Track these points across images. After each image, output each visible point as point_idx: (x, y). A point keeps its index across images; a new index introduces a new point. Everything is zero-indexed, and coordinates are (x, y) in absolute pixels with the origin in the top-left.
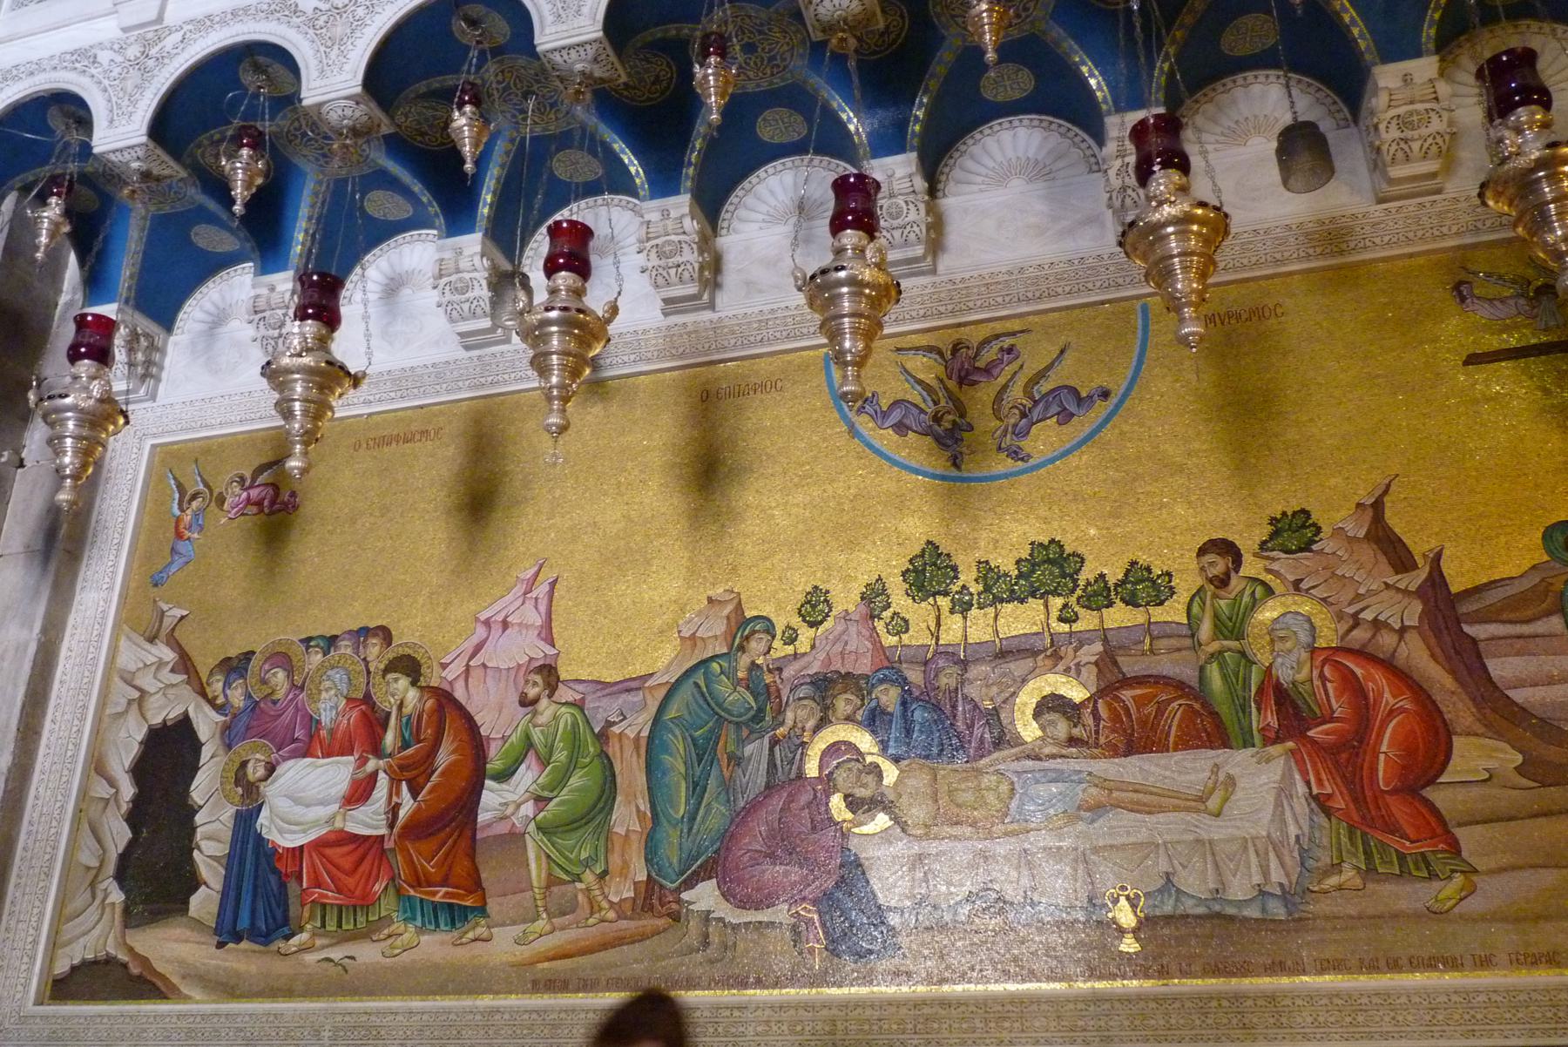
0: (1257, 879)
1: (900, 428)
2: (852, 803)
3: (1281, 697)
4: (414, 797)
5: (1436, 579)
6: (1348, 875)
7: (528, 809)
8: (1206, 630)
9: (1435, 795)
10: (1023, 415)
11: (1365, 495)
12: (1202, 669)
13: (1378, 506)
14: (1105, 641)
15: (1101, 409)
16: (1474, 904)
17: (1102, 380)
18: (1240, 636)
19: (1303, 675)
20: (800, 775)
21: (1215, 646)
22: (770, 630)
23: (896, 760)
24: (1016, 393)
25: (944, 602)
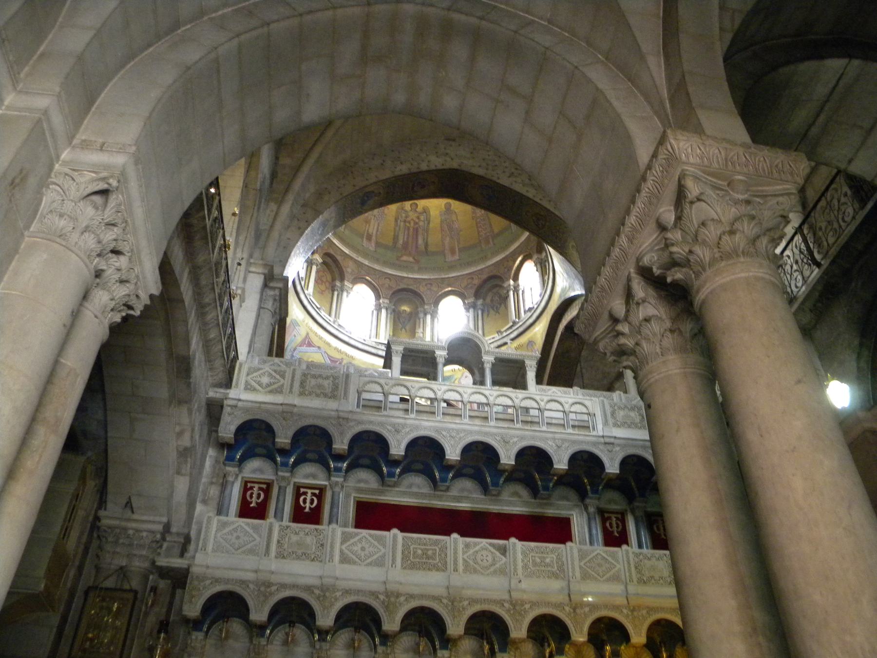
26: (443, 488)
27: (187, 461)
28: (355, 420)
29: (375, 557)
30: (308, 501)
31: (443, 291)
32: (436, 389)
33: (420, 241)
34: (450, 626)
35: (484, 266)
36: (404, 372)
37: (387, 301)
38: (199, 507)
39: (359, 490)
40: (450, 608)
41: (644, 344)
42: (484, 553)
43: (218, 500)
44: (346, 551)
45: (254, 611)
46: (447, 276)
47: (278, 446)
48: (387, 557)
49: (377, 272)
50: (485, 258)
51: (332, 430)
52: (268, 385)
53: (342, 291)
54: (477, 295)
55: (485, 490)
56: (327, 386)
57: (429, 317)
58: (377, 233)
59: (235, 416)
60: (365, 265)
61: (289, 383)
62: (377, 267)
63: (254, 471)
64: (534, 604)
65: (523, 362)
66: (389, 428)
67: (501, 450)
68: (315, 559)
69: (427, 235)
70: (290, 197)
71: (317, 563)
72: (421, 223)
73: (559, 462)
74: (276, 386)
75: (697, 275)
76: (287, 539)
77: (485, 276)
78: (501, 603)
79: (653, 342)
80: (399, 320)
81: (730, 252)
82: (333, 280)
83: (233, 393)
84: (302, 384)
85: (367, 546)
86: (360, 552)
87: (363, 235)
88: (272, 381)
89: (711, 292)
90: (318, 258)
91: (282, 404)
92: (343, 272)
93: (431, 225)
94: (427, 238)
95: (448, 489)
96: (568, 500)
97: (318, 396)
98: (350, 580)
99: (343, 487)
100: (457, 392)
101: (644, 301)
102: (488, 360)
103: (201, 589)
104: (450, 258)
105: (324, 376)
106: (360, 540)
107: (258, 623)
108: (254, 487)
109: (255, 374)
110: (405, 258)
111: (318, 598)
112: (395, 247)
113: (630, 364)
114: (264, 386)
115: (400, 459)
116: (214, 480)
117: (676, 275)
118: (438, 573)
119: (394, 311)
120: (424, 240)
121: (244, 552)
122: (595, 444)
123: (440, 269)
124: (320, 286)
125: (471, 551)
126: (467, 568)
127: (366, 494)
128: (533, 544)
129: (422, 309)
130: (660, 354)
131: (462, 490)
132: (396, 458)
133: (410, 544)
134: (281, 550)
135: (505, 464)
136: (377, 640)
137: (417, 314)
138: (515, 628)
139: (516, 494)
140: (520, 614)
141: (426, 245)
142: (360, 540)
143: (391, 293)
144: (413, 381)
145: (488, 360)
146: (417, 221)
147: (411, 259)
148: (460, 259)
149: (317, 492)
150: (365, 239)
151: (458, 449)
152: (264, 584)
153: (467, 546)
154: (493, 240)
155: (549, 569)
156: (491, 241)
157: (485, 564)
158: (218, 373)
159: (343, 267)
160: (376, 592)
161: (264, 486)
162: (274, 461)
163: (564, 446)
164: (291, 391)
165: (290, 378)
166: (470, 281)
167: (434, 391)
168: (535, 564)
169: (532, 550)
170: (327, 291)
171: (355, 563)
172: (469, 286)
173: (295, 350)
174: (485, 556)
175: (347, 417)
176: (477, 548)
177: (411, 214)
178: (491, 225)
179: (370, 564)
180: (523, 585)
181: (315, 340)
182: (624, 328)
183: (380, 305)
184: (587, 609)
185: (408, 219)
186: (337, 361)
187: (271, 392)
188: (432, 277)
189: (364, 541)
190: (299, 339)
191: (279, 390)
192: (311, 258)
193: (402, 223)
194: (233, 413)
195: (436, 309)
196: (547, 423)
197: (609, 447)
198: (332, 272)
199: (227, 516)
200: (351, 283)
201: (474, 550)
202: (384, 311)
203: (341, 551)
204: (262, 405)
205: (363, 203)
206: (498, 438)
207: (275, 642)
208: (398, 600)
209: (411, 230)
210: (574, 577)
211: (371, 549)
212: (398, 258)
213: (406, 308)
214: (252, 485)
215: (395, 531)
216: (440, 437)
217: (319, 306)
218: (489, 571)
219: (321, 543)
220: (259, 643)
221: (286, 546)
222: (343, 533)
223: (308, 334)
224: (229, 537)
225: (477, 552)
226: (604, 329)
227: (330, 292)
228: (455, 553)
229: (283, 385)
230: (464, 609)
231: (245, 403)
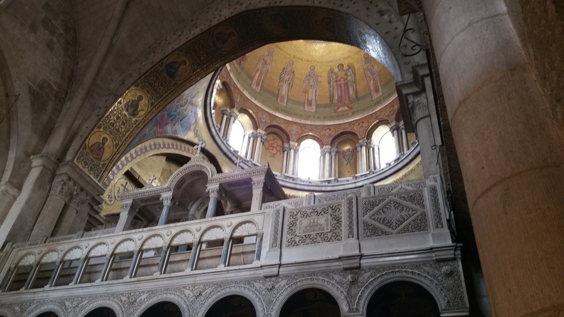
31: (373, 125)
33: (351, 92)
37: (328, 147)
46: (374, 111)
49: (318, 127)
53: (290, 149)
54: (397, 120)
57: (364, 149)
58: (315, 98)
60: (308, 125)
62: (318, 123)
65: (251, 180)
69: (356, 85)
70: (81, 93)
72: (349, 78)
82: (283, 142)
93: (357, 76)
94: (356, 89)
110: (341, 109)
112: (332, 103)
119: (337, 152)
120: (354, 90)
122: (249, 282)
124: (271, 151)
129: (359, 144)
137: (356, 148)
143: (331, 139)
146: (346, 77)
147: (346, 108)
150: (306, 106)
163: (203, 294)
170: (278, 153)
172: (391, 113)
177: (339, 74)
188: (363, 117)
192: (255, 133)
195: (369, 141)
197: (269, 284)
200: (297, 141)
202: (327, 156)
205: (172, 75)
209: (343, 86)
212: (335, 111)
213: (347, 147)
227: (282, 153)
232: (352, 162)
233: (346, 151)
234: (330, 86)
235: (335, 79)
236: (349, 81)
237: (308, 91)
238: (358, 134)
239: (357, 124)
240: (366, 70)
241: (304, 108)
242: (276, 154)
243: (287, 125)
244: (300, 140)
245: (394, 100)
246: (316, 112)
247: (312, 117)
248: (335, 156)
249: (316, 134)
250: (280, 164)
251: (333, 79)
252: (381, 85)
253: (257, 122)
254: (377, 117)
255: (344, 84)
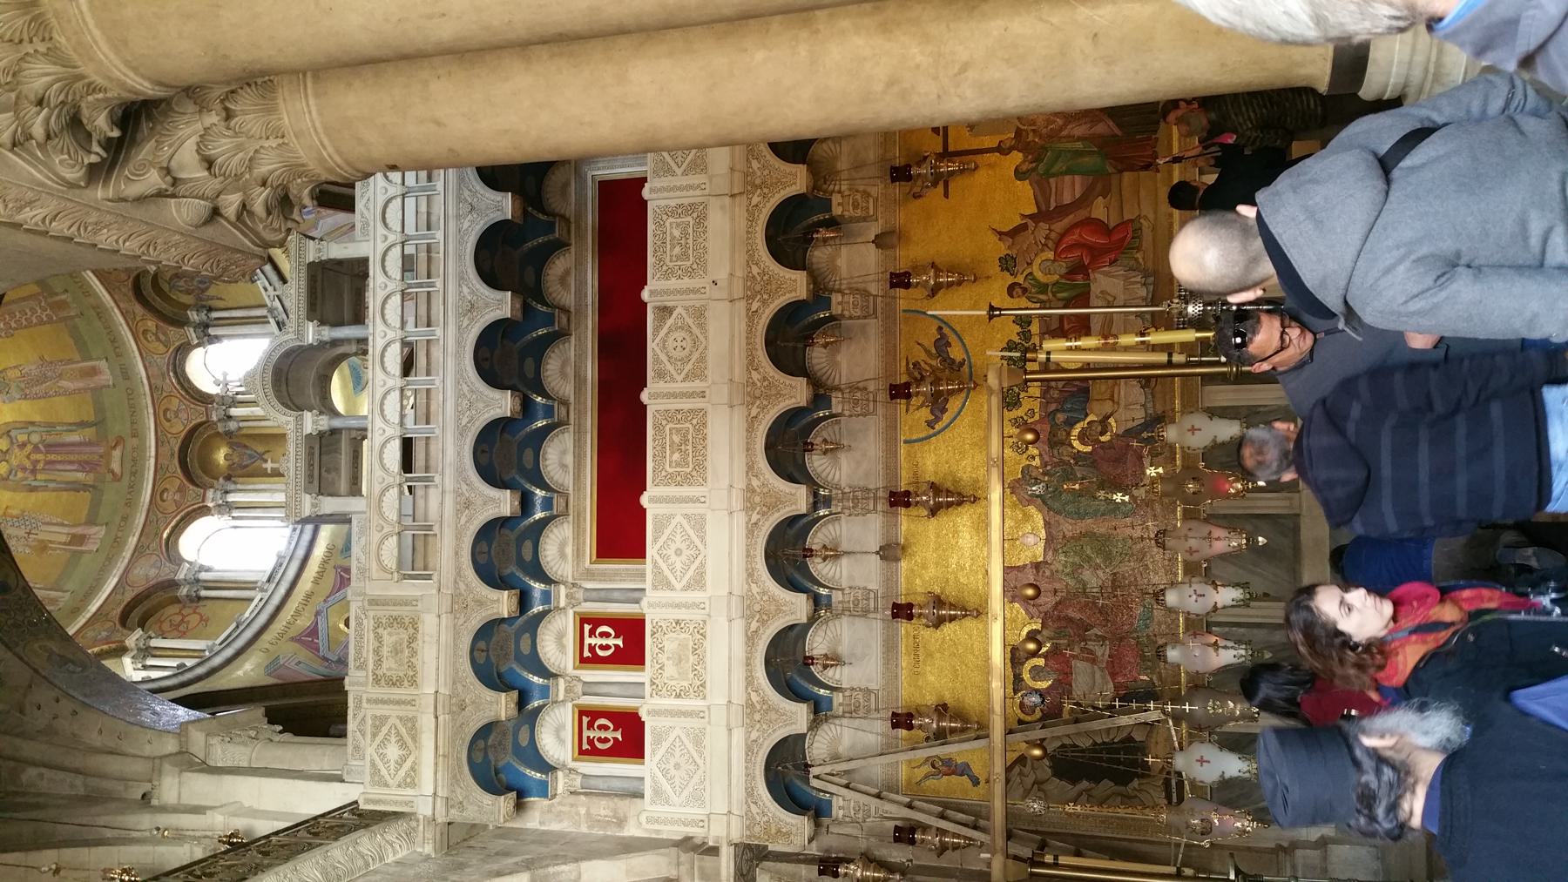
0: (1139, 286)
1: (944, 410)
2: (1102, 434)
3: (1072, 272)
4: (1093, 627)
5: (1031, 217)
6: (1139, 256)
7: (1100, 573)
8: (1043, 297)
9: (1112, 225)
10: (945, 361)
11: (995, 238)
12: (1059, 300)
13: (1000, 233)
14: (1045, 333)
15: (946, 330)
16: (1151, 216)
17: (934, 330)
18: (1047, 285)
19: (1064, 265)
20: (1091, 453)
21: (1050, 294)
22: (1028, 466)
23: (1087, 415)
24: (934, 363)
25: (1022, 395)
26: (563, 410)
27: (554, 873)
28: (455, 582)
29: (691, 532)
30: (604, 642)
32: (383, 439)
33: (75, 437)
34: (793, 400)
35: (116, 310)
36: (355, 489)
37: (210, 494)
38: (632, 831)
39: (578, 553)
40: (765, 403)
41: (263, 169)
42: (670, 344)
43: (616, 799)
44: (684, 582)
45: (794, 726)
46: (145, 381)
47: (513, 711)
48: (689, 512)
49: (152, 517)
50: (100, 311)
51: (476, 622)
52: (402, 744)
53: (198, 581)
54: (181, 322)
55: (561, 335)
56: (394, 638)
57: (234, 412)
58: (66, 525)
59: (467, 797)
61: (396, 707)
62: (140, 519)
63: (561, 741)
64: (751, 259)
65: (311, 265)
66: (463, 520)
67: (487, 317)
68: (701, 631)
71: (708, 628)
72: (35, 438)
73: (500, 209)
74: (403, 731)
75: (92, 88)
76: (673, 683)
77: (139, 309)
78: (752, 316)
79: (256, 151)
80: (247, 466)
81: (28, 17)
82: (177, 600)
83: (424, 809)
84: (393, 683)
85: (674, 547)
86: (684, 558)
87: (75, 551)
88: (393, 739)
89: (135, 70)
90: (133, 639)
91: (437, 717)
92: (158, 584)
93: (37, 418)
94: (70, 424)
95: (565, 403)
96: (566, 185)
97: (414, 653)
98: (730, 571)
99: (574, 585)
100: (384, 397)
101: (167, 171)
102: (312, 333)
103: (765, 819)
104: (106, 377)
105: (377, 644)
106: (665, 558)
107: (812, 717)
108: (589, 737)
109: (384, 772)
110: (116, 466)
111: (763, 622)
112: (91, 486)
113: (306, 191)
114: (404, 752)
115: (518, 495)
116: (583, 811)
117: (101, 124)
118: (709, 424)
119: (228, 478)
120: (71, 431)
121: (701, 754)
123: (131, 394)
124: (190, 627)
125: (669, 367)
126: (698, 373)
127: (584, 543)
128: (650, 260)
130: (280, 141)
131: (563, 374)
132: (517, 503)
133: (664, 473)
134: (691, 690)
135: (512, 310)
136: (821, 513)
137: (229, 434)
138: (790, 292)
139: (563, 280)
140: (769, 282)
141: (82, 424)
142: (665, 558)
143: (191, 487)
144: (370, 481)
145: (312, 333)
146: (29, 448)
147: (117, 453)
148: (107, 360)
149: (587, 628)
150: (83, 548)
151: (491, 396)
152: (750, 715)
153: (661, 375)
154: (57, 294)
155: (691, 231)
156: (57, 298)
157: (688, 344)
158: (387, 842)
159: (147, 586)
160: (747, 527)
161: (585, 720)
162: (540, 709)
164: (410, 703)
165: (386, 706)
166: (151, 337)
167: (387, 441)
168: (685, 256)
169: (660, 260)
170: (201, 610)
171: (702, 565)
172: (162, 338)
173: (325, 659)
174: (675, 344)
175: (449, 597)
176: (663, 357)
177: (14, 462)
178: (24, 299)
179: (702, 539)
180: (722, 275)
181: (304, 622)
182: (231, 203)
183: (219, 506)
184: (755, 164)
185: (28, 464)
186: (341, 576)
187: (414, 739)
188: (151, 410)
189: (665, 552)
190: (304, 654)
191: (410, 725)
193: (39, 477)
194: (461, 803)
195: (217, 400)
196: (429, 228)
198: (162, 605)
199: (643, 779)
200: (179, 565)
201: (667, 363)
202: (231, 498)
203: (687, 588)
204: (441, 752)
206: (466, 322)
207: (837, 677)
208: (758, 490)
209: (52, 457)
210: (703, 186)
211: (678, 538)
213: (221, 456)
214: (585, 740)
215: (645, 500)
216: (473, 429)
217: (234, 625)
218: (701, 338)
219: (674, 624)
220: (840, 704)
221: (686, 684)
222: (655, 588)
223: (292, 639)
224: (677, 781)
225: (670, 358)
226: (235, 231)
227: (201, 603)
228: (674, 395)
229: (401, 719)
230: (765, 379)
231: (440, 783)
232: (260, 449)
233: (230, 462)
234: (45, 489)
235: (27, 474)
236: (42, 441)
237: (43, 541)
238: (194, 422)
239: (167, 424)
240: (26, 395)
241: (90, 552)
242: (202, 617)
243: (127, 588)
244: (178, 560)
245: (131, 329)
246: (107, 524)
247: (120, 534)
248: (235, 483)
249: (169, 523)
250: (231, 605)
251: (26, 479)
252: (78, 362)
253: (105, 647)
254: (163, 375)
255: (48, 452)
